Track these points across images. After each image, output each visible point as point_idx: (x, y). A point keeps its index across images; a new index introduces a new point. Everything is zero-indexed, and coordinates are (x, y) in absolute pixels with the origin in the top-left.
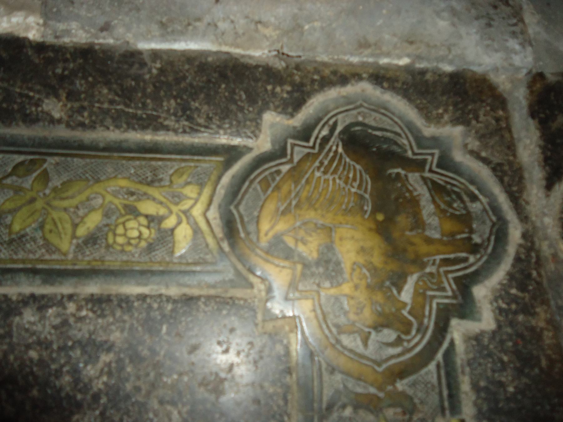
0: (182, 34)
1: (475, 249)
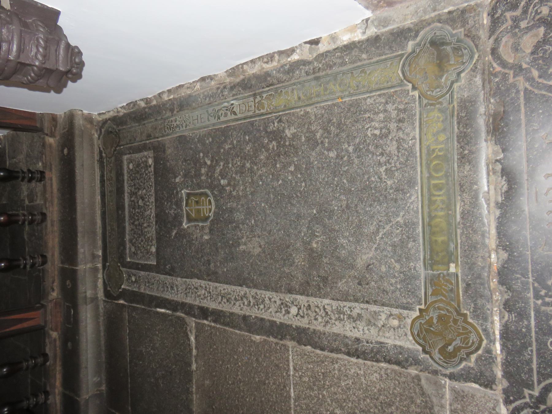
0: (387, 26)
1: (463, 63)
